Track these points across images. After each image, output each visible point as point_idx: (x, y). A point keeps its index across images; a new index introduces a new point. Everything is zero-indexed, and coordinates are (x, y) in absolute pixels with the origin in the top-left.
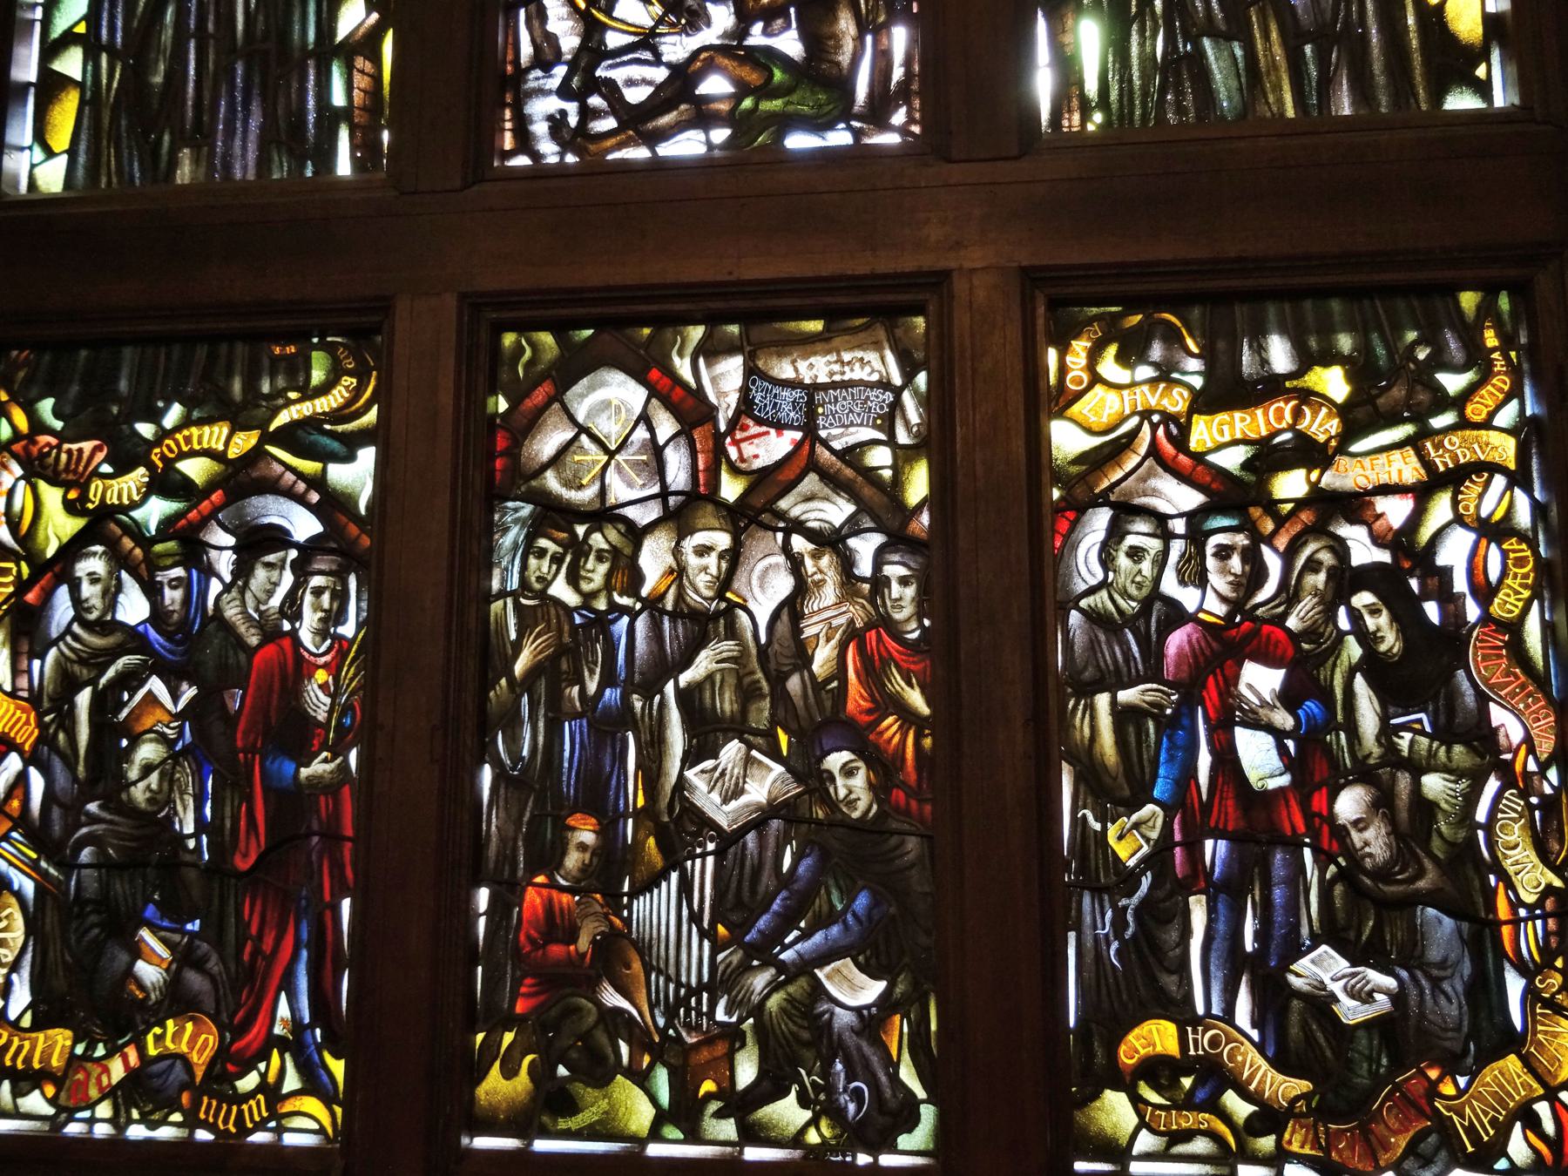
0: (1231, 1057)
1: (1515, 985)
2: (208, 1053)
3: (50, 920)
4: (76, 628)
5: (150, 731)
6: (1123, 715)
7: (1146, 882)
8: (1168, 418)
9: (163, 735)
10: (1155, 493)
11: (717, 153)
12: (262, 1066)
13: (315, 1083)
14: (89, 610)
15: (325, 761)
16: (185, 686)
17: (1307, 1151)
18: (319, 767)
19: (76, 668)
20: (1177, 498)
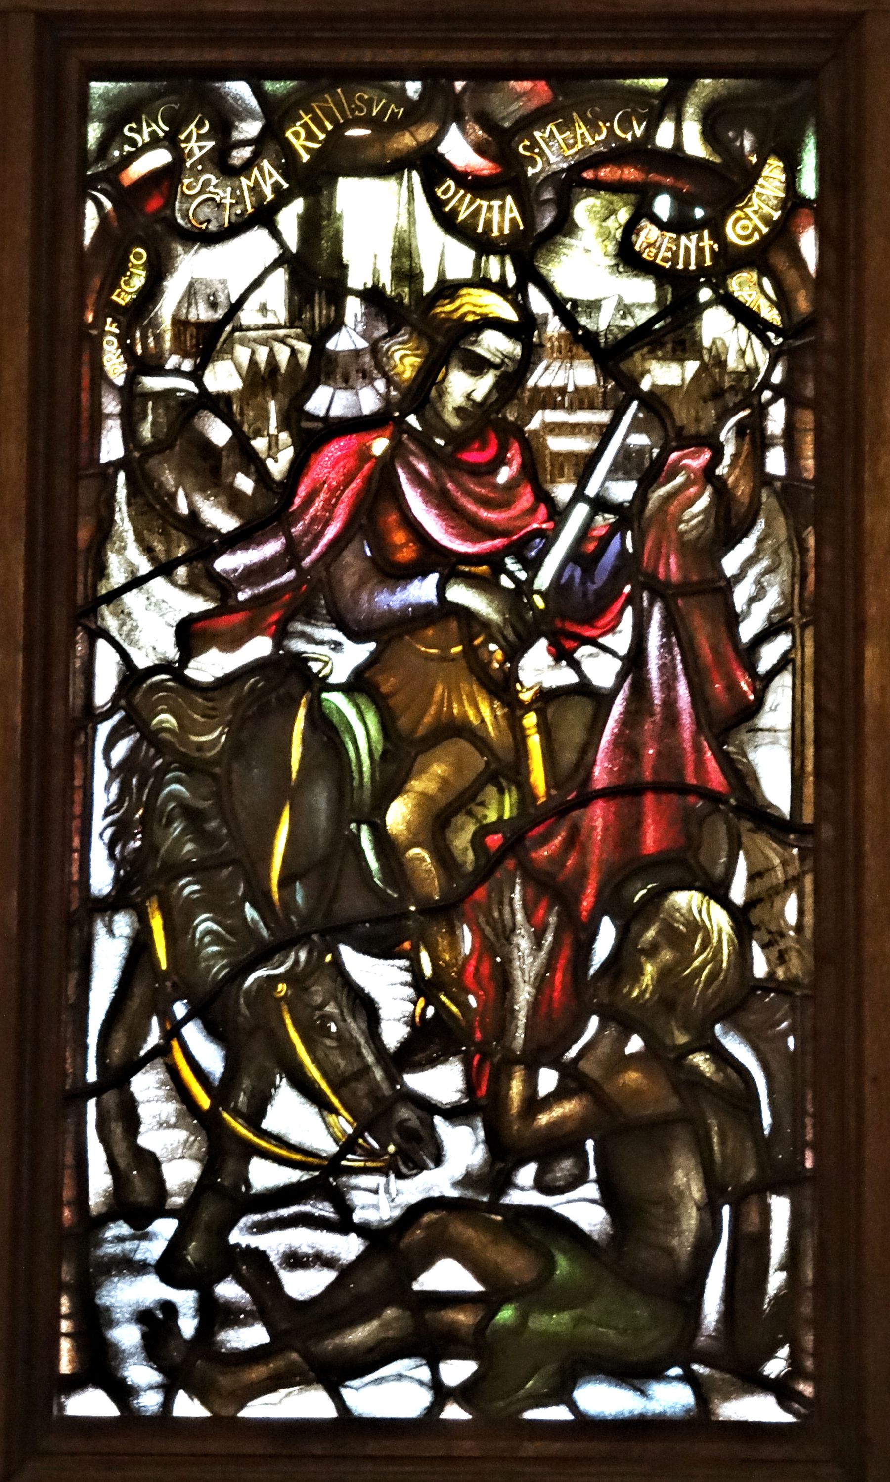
11: (453, 1412)
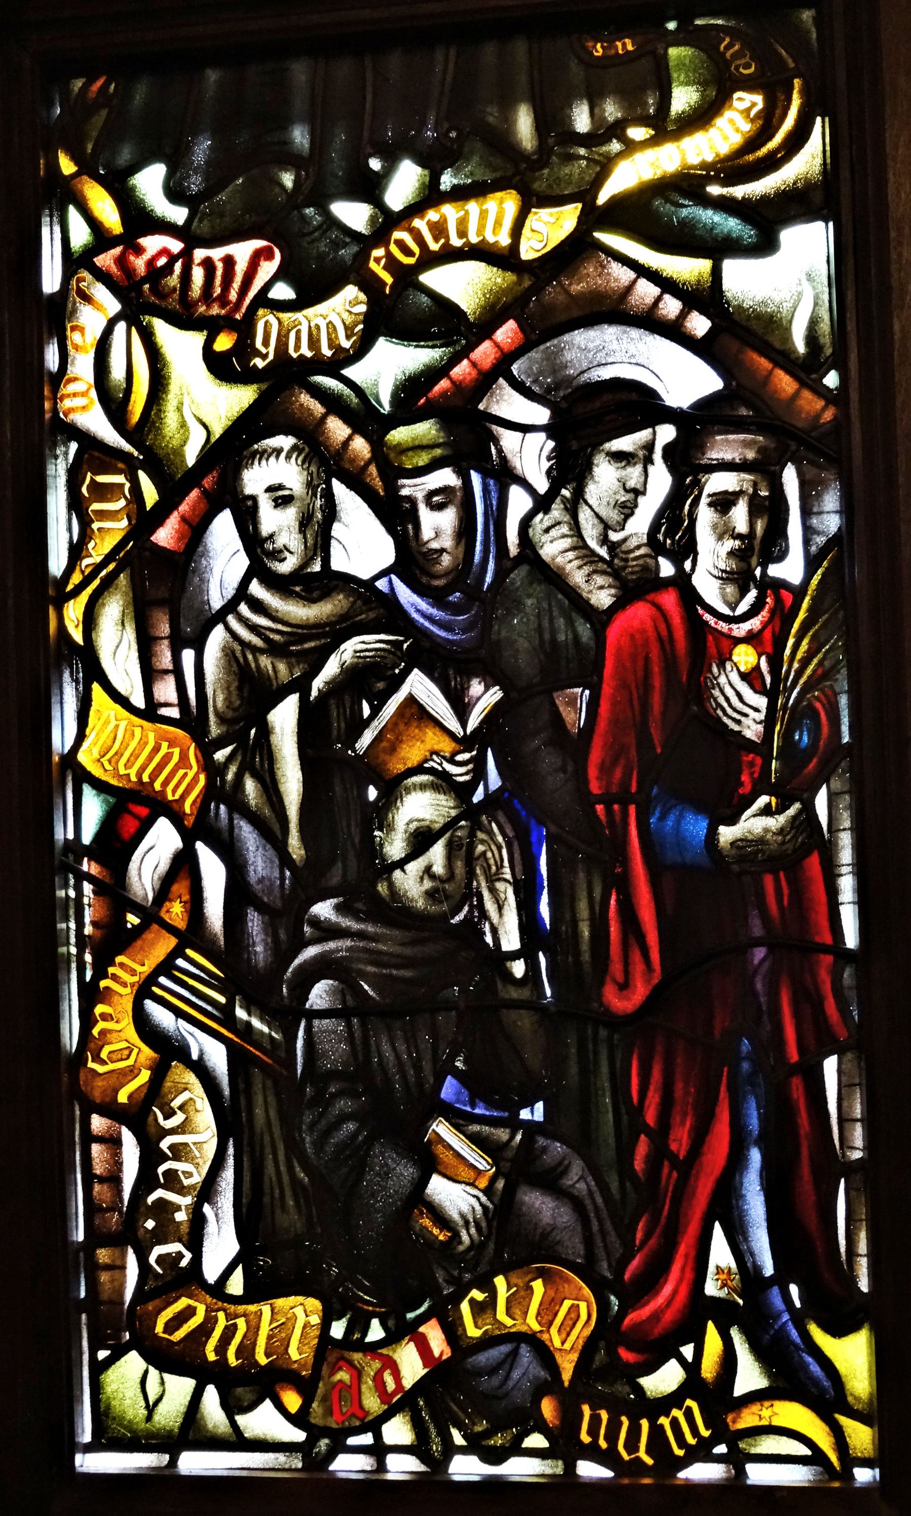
2: (581, 1331)
3: (263, 1111)
4: (256, 588)
5: (419, 769)
9: (445, 776)
12: (688, 1351)
13: (800, 1378)
14: (278, 555)
15: (767, 811)
16: (476, 687)
18: (754, 824)
19: (265, 661)
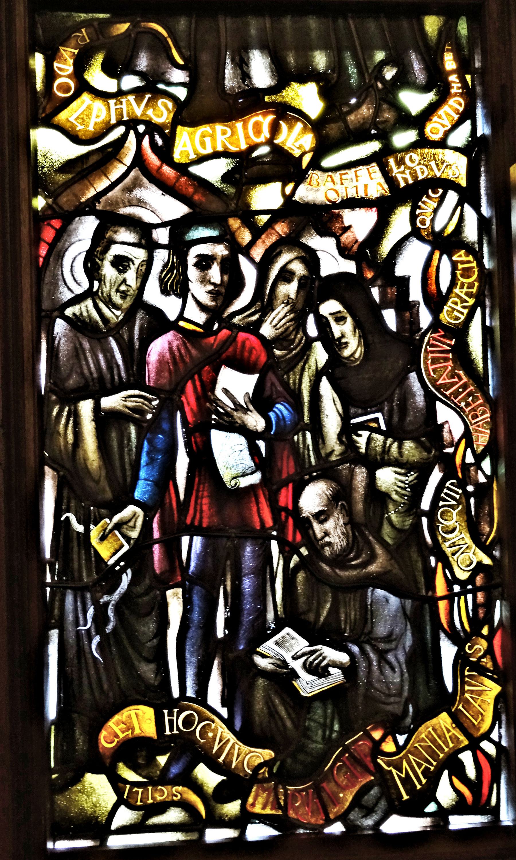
0: (203, 733)
1: (448, 651)
6: (104, 420)
7: (126, 579)
8: (152, 128)
10: (140, 203)
17: (268, 811)
20: (162, 207)
